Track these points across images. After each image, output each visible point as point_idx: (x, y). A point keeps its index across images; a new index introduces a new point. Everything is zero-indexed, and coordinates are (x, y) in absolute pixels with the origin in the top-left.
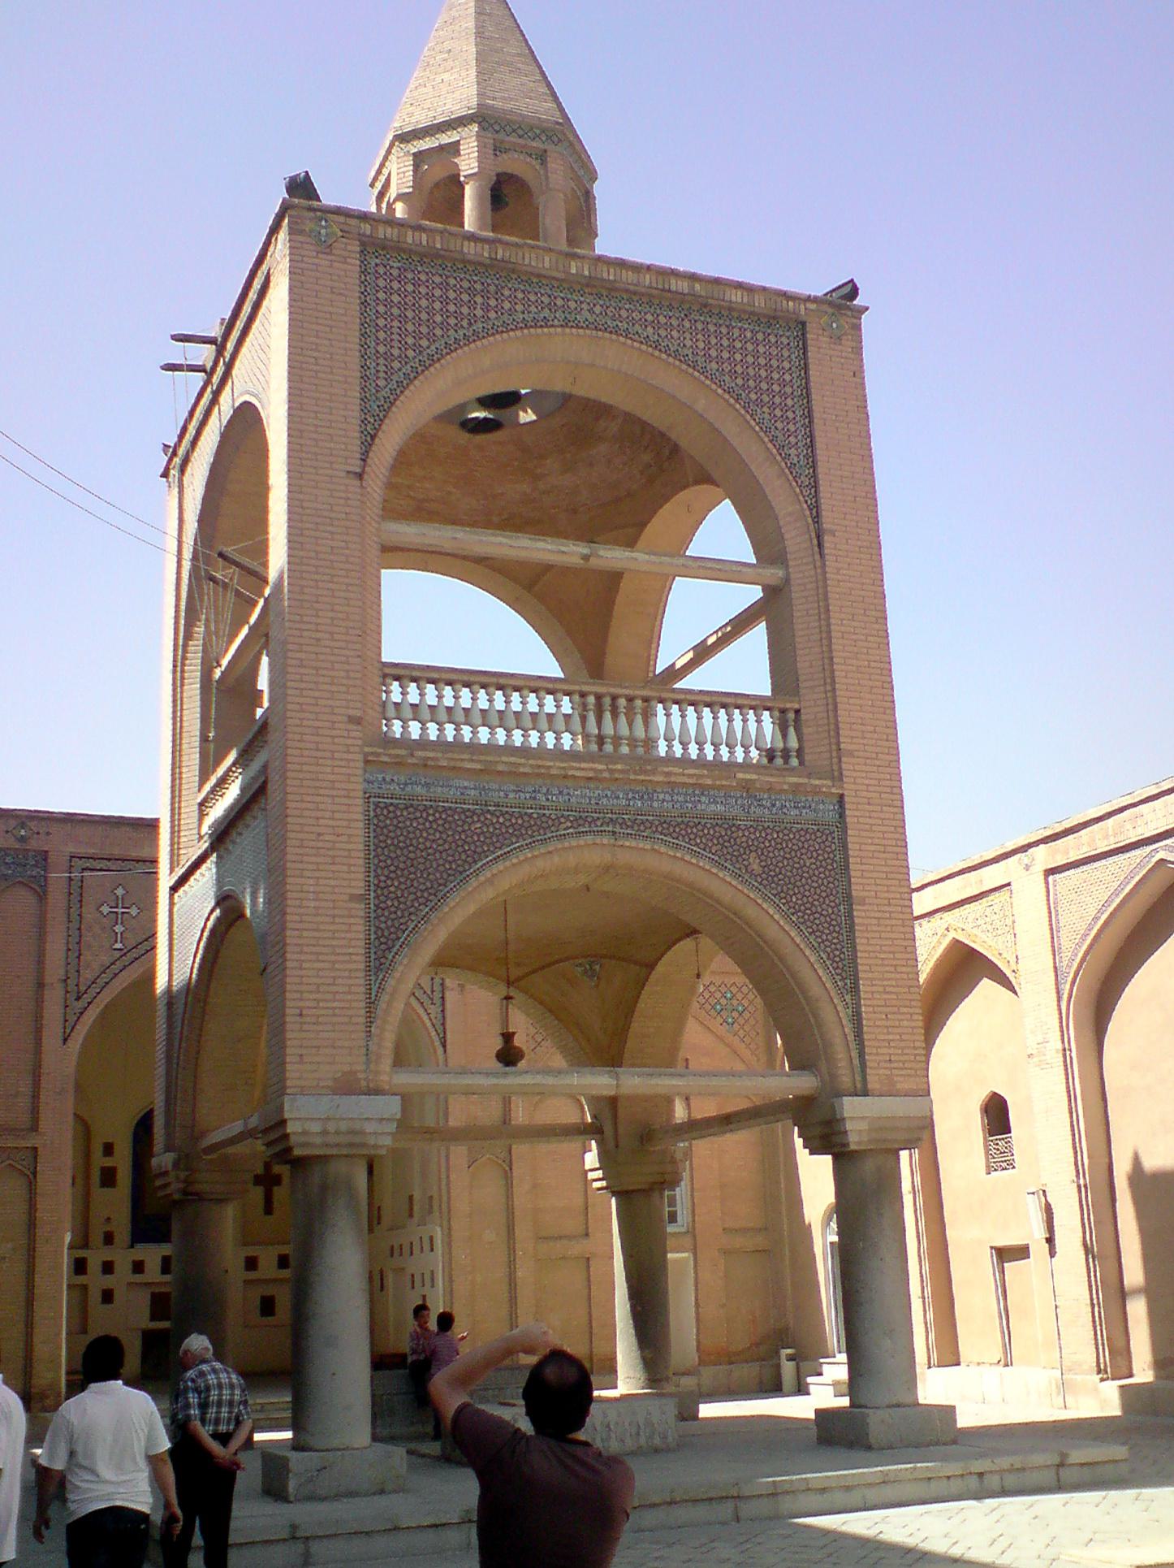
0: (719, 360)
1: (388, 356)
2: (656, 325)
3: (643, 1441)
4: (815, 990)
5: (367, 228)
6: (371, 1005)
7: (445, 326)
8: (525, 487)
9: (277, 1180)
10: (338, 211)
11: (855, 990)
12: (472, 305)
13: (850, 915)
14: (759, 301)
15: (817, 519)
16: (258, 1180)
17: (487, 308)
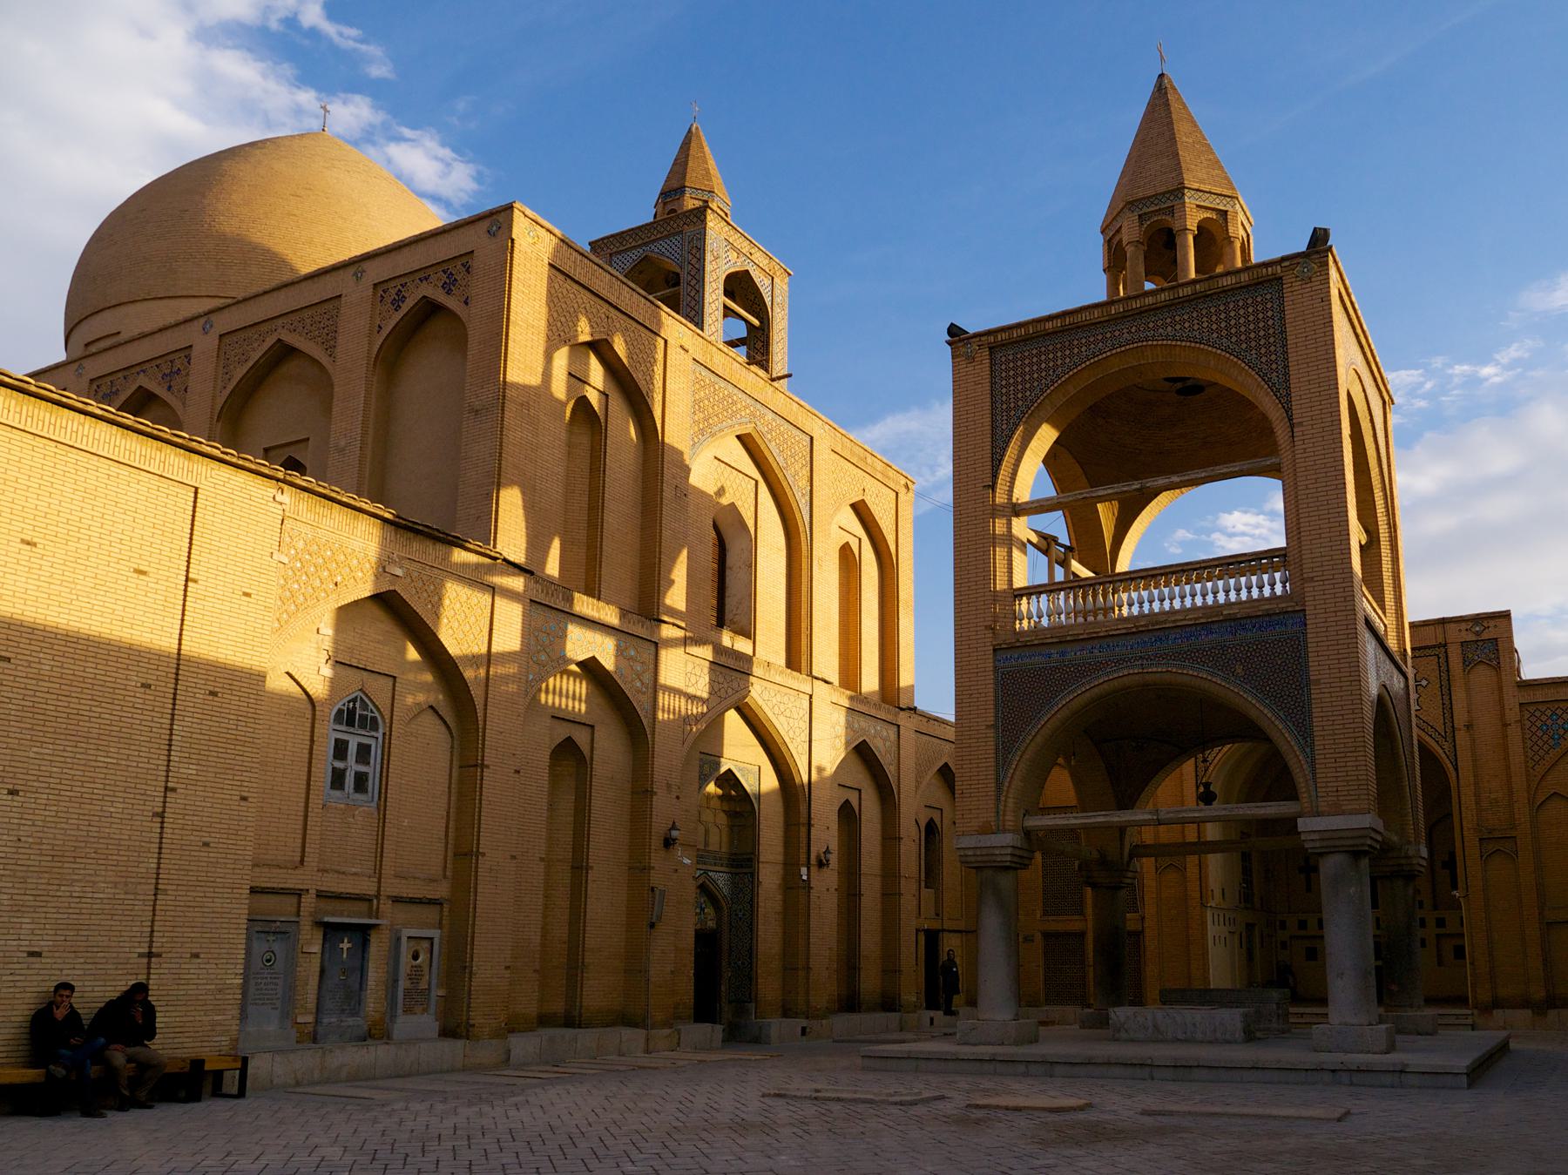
5: (992, 339)
7: (1039, 380)
10: (976, 335)
12: (1055, 359)
17: (1063, 358)
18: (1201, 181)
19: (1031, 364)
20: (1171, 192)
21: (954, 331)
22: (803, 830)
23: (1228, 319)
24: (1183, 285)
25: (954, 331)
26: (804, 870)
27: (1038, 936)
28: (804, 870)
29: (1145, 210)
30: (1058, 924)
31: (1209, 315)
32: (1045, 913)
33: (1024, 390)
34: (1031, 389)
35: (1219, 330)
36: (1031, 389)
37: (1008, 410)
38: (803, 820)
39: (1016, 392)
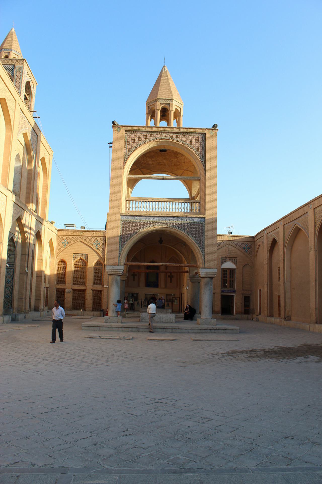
0: (189, 142)
1: (129, 149)
2: (177, 137)
3: (169, 321)
4: (197, 251)
5: (126, 128)
6: (120, 252)
7: (139, 142)
8: (176, 159)
9: (173, 277)
10: (121, 126)
11: (204, 251)
12: (144, 138)
13: (205, 238)
14: (197, 131)
15: (205, 169)
16: (169, 276)
18: (176, 99)
19: (137, 138)
20: (170, 99)
21: (113, 123)
22: (27, 256)
23: (191, 140)
24: (181, 128)
25: (113, 123)
26: (26, 269)
27: (72, 290)
28: (26, 269)
29: (162, 102)
30: (76, 287)
31: (186, 137)
32: (74, 284)
33: (134, 145)
34: (136, 145)
35: (189, 142)
36: (136, 145)
37: (129, 149)
38: (27, 253)
39: (132, 144)
